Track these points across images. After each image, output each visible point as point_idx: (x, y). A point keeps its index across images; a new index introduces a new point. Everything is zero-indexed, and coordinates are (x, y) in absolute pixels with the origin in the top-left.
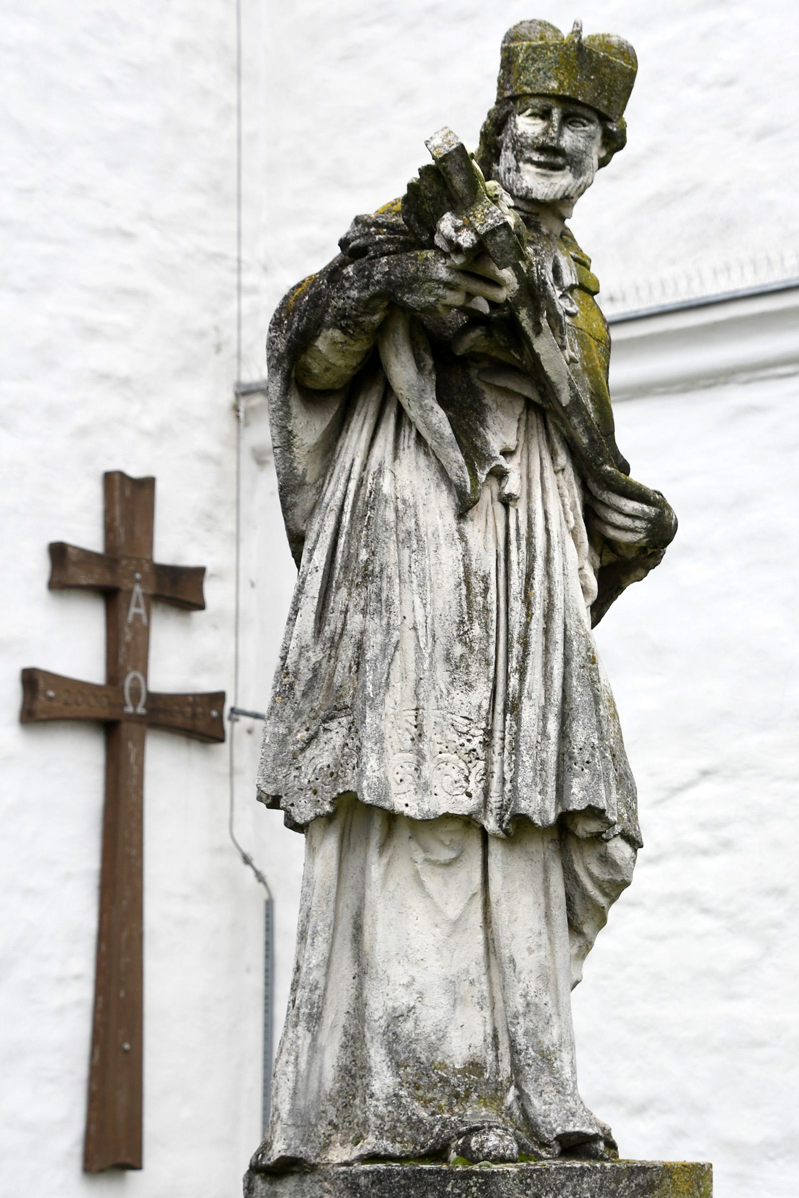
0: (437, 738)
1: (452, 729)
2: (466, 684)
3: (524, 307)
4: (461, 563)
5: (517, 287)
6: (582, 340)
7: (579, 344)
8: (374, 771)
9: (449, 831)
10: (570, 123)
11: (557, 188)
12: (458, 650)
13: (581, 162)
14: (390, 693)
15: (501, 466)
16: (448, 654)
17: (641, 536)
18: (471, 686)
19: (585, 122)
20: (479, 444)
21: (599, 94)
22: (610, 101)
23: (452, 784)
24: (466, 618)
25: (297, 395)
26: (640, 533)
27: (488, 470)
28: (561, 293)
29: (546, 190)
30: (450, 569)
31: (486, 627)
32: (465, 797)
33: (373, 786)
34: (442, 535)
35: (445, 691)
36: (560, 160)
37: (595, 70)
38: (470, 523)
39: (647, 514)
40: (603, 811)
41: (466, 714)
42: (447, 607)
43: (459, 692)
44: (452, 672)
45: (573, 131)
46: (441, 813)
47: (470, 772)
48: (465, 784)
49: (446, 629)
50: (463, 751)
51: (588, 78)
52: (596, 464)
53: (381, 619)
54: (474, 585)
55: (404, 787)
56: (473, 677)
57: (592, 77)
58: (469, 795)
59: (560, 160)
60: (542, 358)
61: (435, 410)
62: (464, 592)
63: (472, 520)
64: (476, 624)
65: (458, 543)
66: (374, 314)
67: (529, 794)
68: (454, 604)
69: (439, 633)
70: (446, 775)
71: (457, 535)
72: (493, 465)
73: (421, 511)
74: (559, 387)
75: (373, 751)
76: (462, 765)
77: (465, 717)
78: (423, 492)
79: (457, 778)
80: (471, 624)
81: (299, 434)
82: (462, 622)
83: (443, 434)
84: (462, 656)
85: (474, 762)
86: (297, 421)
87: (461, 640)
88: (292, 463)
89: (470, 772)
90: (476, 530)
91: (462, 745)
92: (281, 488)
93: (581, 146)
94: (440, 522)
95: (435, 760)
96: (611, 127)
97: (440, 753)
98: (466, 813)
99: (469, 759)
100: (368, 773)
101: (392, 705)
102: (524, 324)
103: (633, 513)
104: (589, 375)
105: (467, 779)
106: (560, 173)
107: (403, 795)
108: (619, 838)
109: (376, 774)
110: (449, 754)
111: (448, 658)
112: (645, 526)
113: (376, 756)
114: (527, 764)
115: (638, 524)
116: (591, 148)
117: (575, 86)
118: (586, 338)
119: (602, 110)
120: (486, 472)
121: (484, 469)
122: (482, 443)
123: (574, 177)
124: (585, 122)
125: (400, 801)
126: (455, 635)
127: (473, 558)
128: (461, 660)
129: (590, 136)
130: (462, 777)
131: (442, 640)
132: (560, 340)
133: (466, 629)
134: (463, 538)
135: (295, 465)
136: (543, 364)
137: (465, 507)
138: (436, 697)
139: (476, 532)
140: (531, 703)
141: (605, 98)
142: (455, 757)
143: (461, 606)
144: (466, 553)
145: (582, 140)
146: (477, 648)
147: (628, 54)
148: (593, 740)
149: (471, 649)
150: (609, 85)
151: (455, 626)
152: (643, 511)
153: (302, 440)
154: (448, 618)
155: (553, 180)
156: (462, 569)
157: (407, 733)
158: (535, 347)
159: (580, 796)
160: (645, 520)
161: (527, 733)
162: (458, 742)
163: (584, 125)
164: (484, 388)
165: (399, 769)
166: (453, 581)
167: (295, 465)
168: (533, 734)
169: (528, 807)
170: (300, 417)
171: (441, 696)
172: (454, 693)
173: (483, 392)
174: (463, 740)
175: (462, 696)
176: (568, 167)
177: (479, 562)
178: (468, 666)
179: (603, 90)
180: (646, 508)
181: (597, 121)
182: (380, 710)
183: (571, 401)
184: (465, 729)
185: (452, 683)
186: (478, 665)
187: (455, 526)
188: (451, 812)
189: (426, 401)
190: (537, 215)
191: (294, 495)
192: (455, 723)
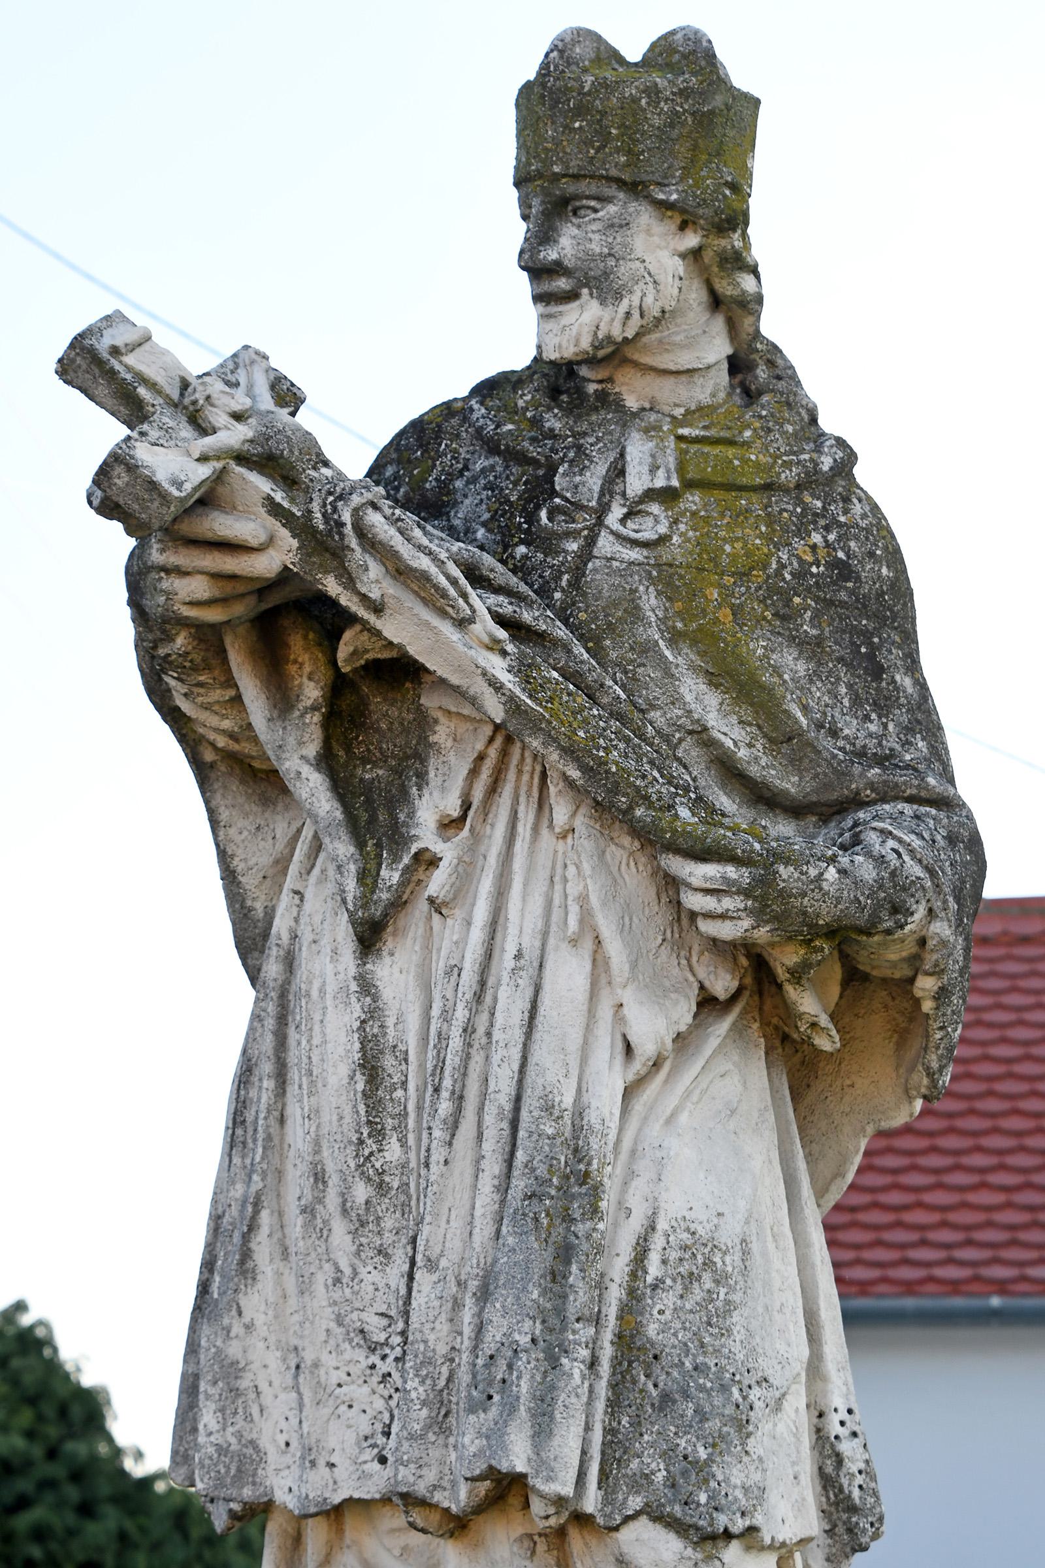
0: (329, 1360)
1: (358, 1339)
2: (380, 1252)
3: (326, 572)
4: (356, 1035)
5: (295, 543)
6: (669, 584)
7: (659, 593)
8: (211, 1434)
9: (393, 1531)
10: (575, 213)
11: (575, 329)
12: (361, 1192)
13: (606, 274)
14: (259, 1286)
15: (427, 849)
16: (344, 1202)
17: (746, 923)
18: (387, 1256)
19: (592, 203)
20: (402, 817)
21: (598, 151)
22: (629, 152)
23: (358, 1443)
24: (365, 1135)
25: (234, 785)
26: (739, 918)
27: (406, 860)
28: (625, 510)
29: (556, 340)
30: (341, 1051)
31: (403, 1142)
32: (376, 1466)
33: (207, 1462)
34: (331, 988)
35: (348, 1271)
36: (563, 284)
37: (581, 111)
38: (387, 960)
39: (734, 882)
40: (522, 1477)
41: (383, 1308)
42: (335, 1118)
43: (370, 1268)
44: (354, 1233)
45: (579, 227)
46: (337, 1499)
47: (392, 1417)
48: (381, 1440)
49: (337, 1160)
50: (376, 1379)
51: (568, 128)
52: (619, 810)
53: (243, 1157)
54: (391, 1071)
55: (288, 1459)
56: (388, 1238)
57: (577, 125)
58: (383, 1460)
59: (563, 284)
60: (411, 650)
61: (304, 776)
62: (360, 1086)
63: (392, 954)
64: (394, 1139)
65: (353, 999)
66: (173, 640)
67: (417, 1454)
68: (347, 1110)
69: (330, 1167)
70: (349, 1427)
71: (354, 987)
72: (413, 850)
73: (305, 952)
74: (472, 692)
75: (208, 1397)
76: (379, 1404)
77: (382, 1314)
78: (317, 919)
79: (366, 1429)
80: (379, 1142)
81: (239, 852)
82: (361, 1142)
83: (317, 816)
84: (367, 1202)
85: (396, 1396)
86: (232, 832)
87: (363, 1173)
88: (244, 901)
89: (392, 1417)
90: (396, 969)
91: (373, 1367)
92: (238, 945)
93: (596, 246)
94: (329, 969)
95: (331, 1402)
96: (661, 196)
97: (340, 1385)
98: (377, 1496)
99: (386, 1394)
100: (202, 1439)
101: (263, 1308)
102: (343, 601)
103: (708, 885)
104: (694, 643)
105: (387, 1434)
106: (575, 305)
107: (286, 1472)
108: (644, 1519)
109: (212, 1439)
110: (353, 1387)
111: (345, 1212)
112: (742, 906)
113: (213, 1406)
114: (414, 1395)
115: (728, 903)
116: (625, 246)
117: (546, 150)
118: (681, 577)
119: (614, 172)
120: (401, 866)
121: (396, 859)
122: (408, 816)
123: (603, 302)
124: (592, 203)
125: (283, 1482)
126: (352, 1165)
127: (390, 1022)
128: (367, 1210)
129: (612, 226)
130: (379, 1427)
131: (334, 1181)
132: (450, 610)
133: (366, 1153)
134: (366, 986)
135: (249, 903)
136: (421, 659)
137: (370, 936)
138: (326, 1286)
139: (397, 974)
140: (435, 1277)
141: (618, 150)
142: (366, 1389)
143: (357, 1112)
144: (373, 1013)
145: (596, 237)
146: (395, 1185)
147: (686, 58)
148: (517, 1337)
149: (382, 1188)
150: (621, 126)
151: (351, 1150)
152: (724, 878)
153: (245, 860)
154: (339, 1137)
155: (565, 321)
156: (357, 1046)
157: (293, 1355)
158: (386, 633)
159: (473, 1449)
160: (738, 893)
161: (418, 1336)
162: (365, 1363)
163: (596, 211)
164: (439, 714)
165: (283, 1424)
166: (344, 1070)
167: (249, 903)
168: (432, 1337)
169: (412, 1479)
170: (241, 823)
171: (337, 1281)
172: (363, 1271)
173: (436, 721)
174: (375, 1359)
175: (376, 1276)
176: (585, 291)
177: (400, 1027)
178: (378, 1219)
179: (606, 138)
180: (731, 871)
181: (621, 195)
182: (226, 1321)
183: (506, 712)
184: (382, 1337)
185: (358, 1253)
186: (398, 1214)
187: (353, 971)
188: (356, 1495)
189: (287, 764)
190: (610, 380)
191: (256, 954)
192: (367, 1328)
